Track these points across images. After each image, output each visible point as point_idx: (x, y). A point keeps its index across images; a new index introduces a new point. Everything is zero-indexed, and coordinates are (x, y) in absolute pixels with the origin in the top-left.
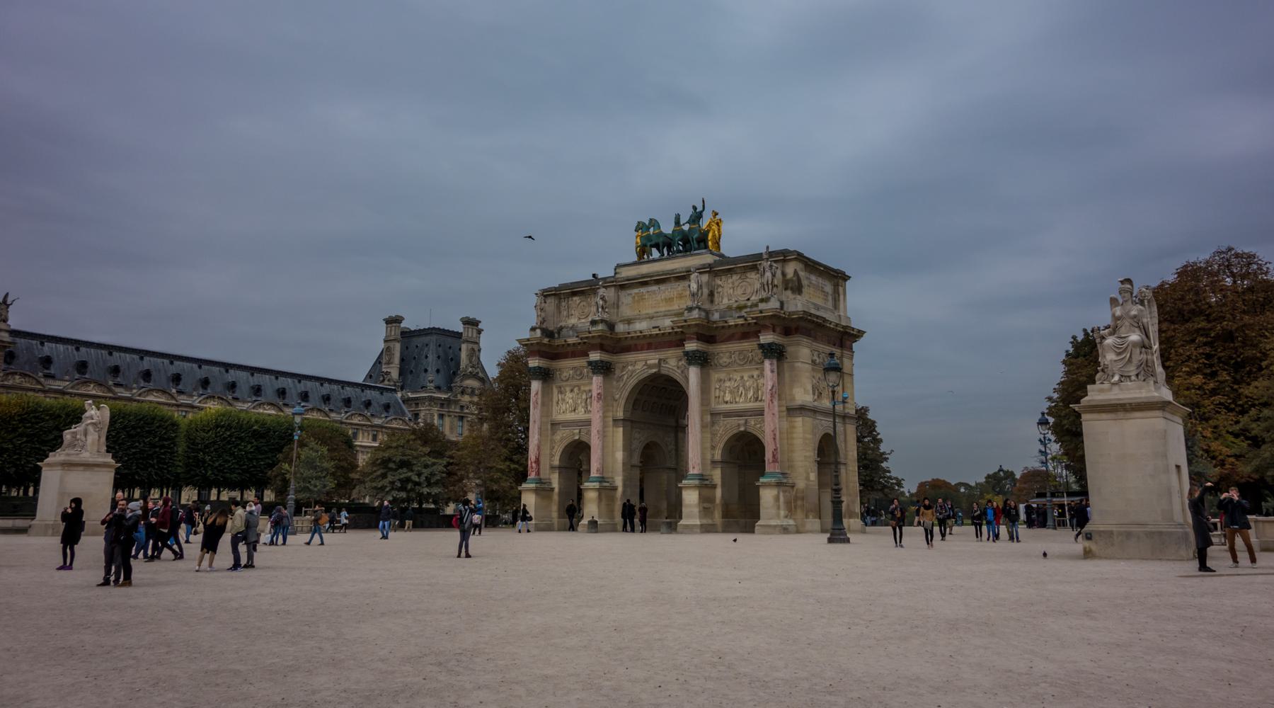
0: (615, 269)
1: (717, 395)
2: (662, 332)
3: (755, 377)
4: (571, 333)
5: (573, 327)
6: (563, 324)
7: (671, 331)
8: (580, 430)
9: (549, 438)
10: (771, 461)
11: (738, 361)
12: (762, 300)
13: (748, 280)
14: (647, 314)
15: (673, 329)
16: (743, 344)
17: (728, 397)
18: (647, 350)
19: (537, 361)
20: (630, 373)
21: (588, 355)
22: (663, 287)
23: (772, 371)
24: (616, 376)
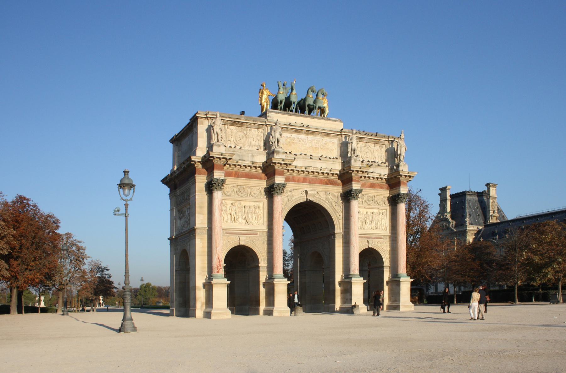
3: (375, 214)
7: (328, 172)
13: (369, 148)
18: (303, 182)
22: (310, 137)
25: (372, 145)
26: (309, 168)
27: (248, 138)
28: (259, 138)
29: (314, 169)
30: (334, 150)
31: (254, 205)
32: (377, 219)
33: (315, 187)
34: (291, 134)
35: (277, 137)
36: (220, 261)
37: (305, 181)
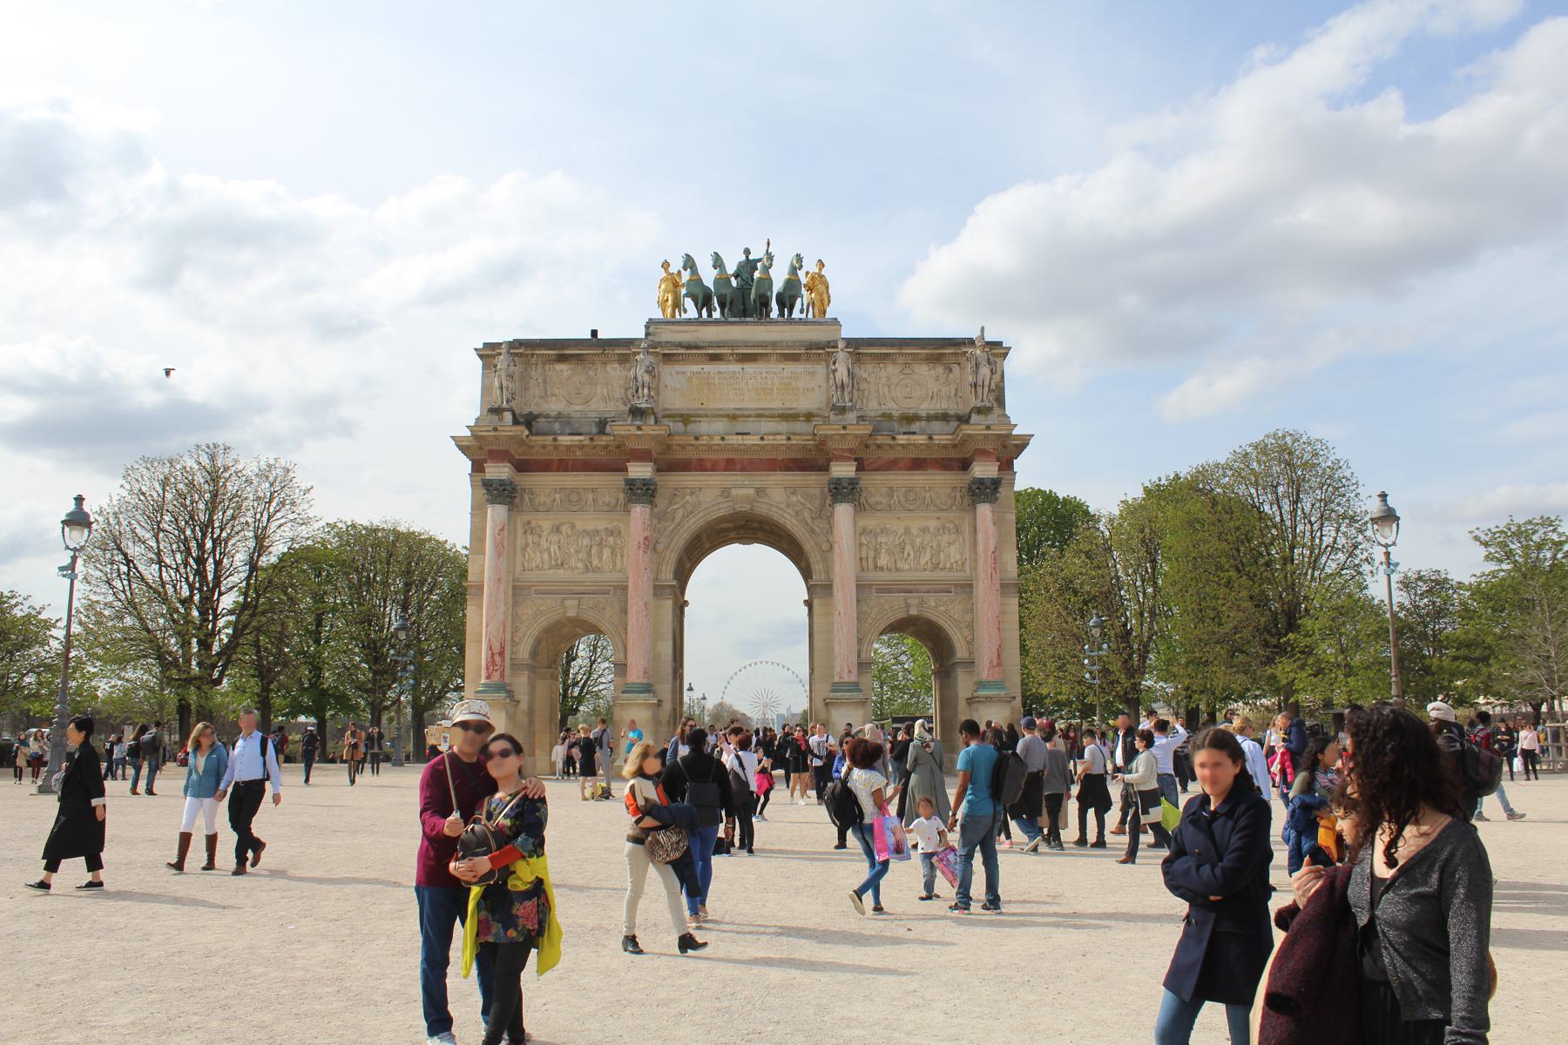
0: (647, 327)
1: (864, 555)
2: (765, 442)
3: (932, 530)
4: (557, 426)
5: (559, 416)
6: (536, 410)
7: (784, 442)
8: (579, 600)
9: (510, 611)
10: (995, 663)
11: (903, 502)
12: (979, 411)
13: (916, 377)
14: (721, 409)
15: (789, 439)
16: (916, 477)
17: (883, 560)
18: (725, 470)
19: (507, 470)
20: (689, 509)
21: (625, 470)
22: (750, 368)
23: (994, 524)
24: (656, 510)
25: (924, 371)
26: (730, 437)
27: (596, 385)
28: (621, 382)
29: (745, 437)
30: (813, 389)
31: (606, 529)
32: (935, 545)
33: (757, 478)
34: (702, 366)
35: (640, 379)
36: (493, 654)
37: (730, 465)
